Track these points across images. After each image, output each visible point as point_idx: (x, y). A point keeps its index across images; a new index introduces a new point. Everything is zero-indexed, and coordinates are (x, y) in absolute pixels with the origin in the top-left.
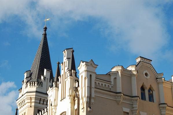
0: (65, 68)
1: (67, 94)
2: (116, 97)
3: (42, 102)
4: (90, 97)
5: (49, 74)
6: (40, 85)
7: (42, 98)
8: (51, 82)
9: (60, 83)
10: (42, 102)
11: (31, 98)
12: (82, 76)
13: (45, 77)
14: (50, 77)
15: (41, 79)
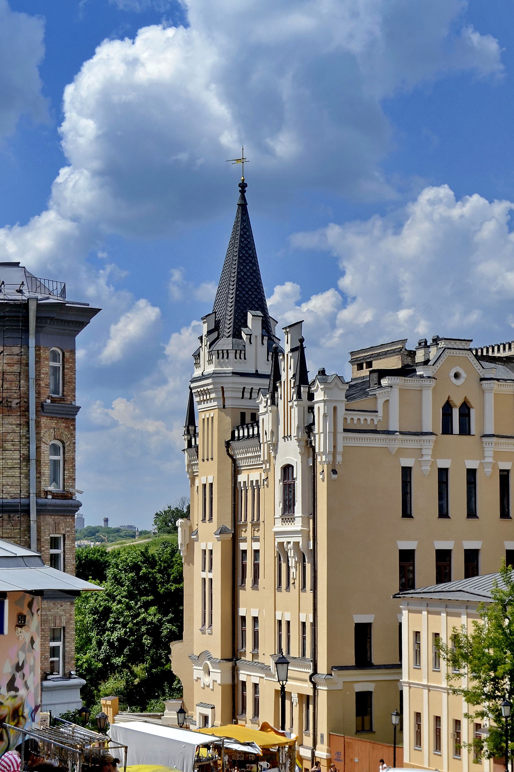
0: (289, 370)
1: (294, 433)
2: (388, 441)
3: (247, 395)
4: (334, 454)
5: (259, 321)
6: (240, 358)
7: (247, 387)
8: (265, 342)
9: (281, 398)
10: (247, 395)
11: (223, 388)
12: (319, 407)
13: (251, 335)
14: (263, 328)
15: (241, 338)
